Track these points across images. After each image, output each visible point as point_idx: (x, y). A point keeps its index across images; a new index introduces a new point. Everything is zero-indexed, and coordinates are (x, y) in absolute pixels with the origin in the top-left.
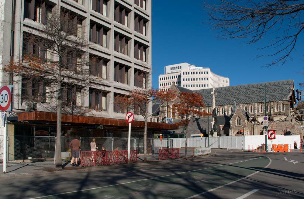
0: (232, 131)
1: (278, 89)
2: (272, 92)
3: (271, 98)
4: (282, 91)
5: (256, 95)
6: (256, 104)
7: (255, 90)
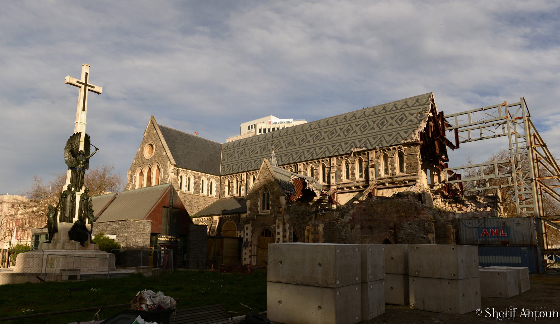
0: (250, 228)
1: (392, 118)
2: (375, 126)
3: (370, 142)
4: (400, 123)
5: (338, 138)
6: (335, 158)
7: (337, 128)
